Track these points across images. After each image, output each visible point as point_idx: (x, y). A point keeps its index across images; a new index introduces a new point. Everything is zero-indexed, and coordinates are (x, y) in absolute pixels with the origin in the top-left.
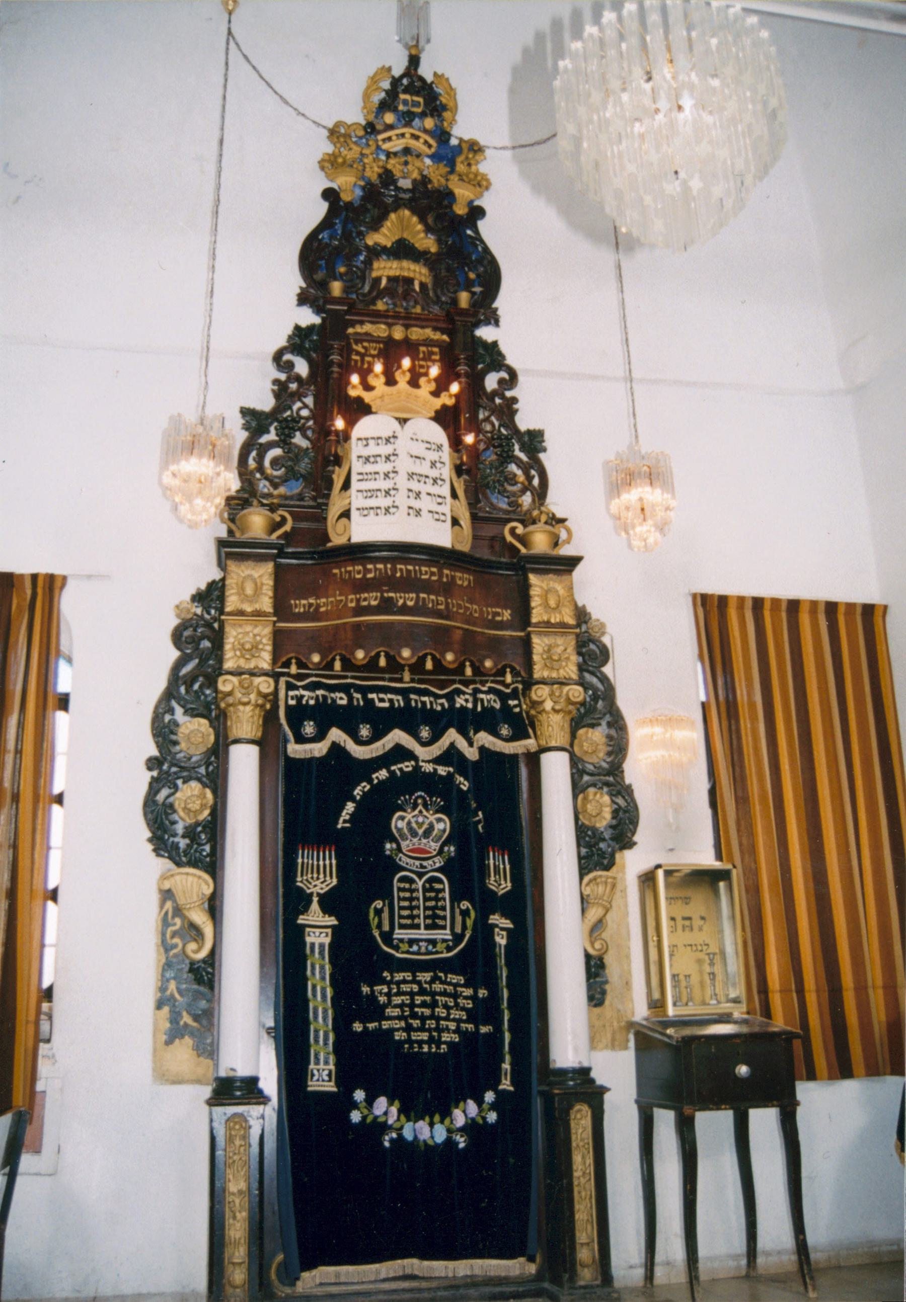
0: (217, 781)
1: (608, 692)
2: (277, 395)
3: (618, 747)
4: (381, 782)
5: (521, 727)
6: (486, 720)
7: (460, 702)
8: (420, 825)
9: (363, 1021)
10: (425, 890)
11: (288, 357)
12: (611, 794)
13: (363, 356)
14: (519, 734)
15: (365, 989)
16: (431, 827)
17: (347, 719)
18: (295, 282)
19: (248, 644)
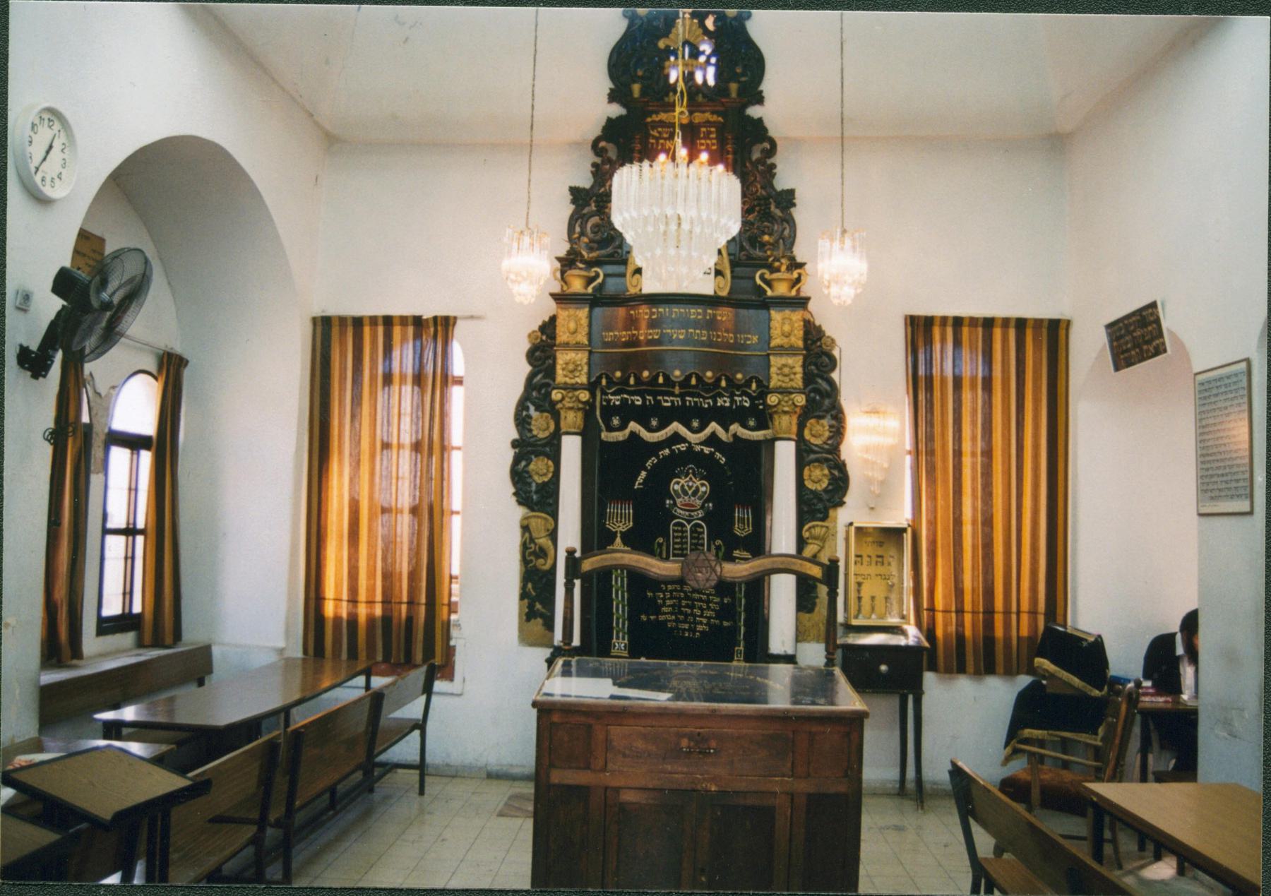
0: (556, 457)
1: (833, 391)
2: (594, 174)
3: (838, 432)
4: (654, 466)
5: (763, 418)
6: (739, 415)
7: (720, 402)
8: (690, 488)
9: (648, 615)
10: (692, 532)
11: (602, 144)
12: (830, 468)
13: (657, 139)
14: (762, 425)
15: (649, 594)
16: (697, 489)
17: (642, 416)
18: (606, 85)
19: (572, 365)
